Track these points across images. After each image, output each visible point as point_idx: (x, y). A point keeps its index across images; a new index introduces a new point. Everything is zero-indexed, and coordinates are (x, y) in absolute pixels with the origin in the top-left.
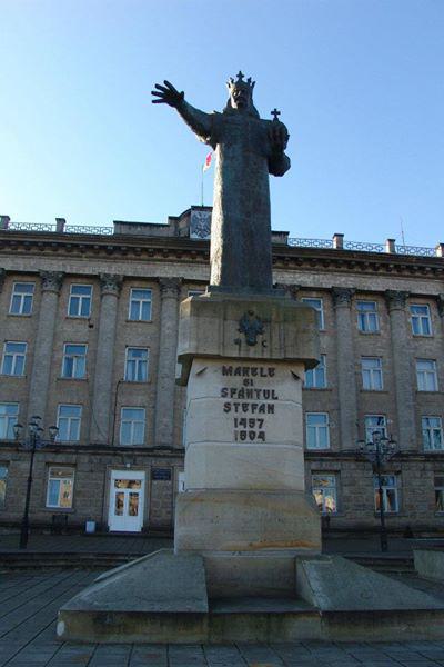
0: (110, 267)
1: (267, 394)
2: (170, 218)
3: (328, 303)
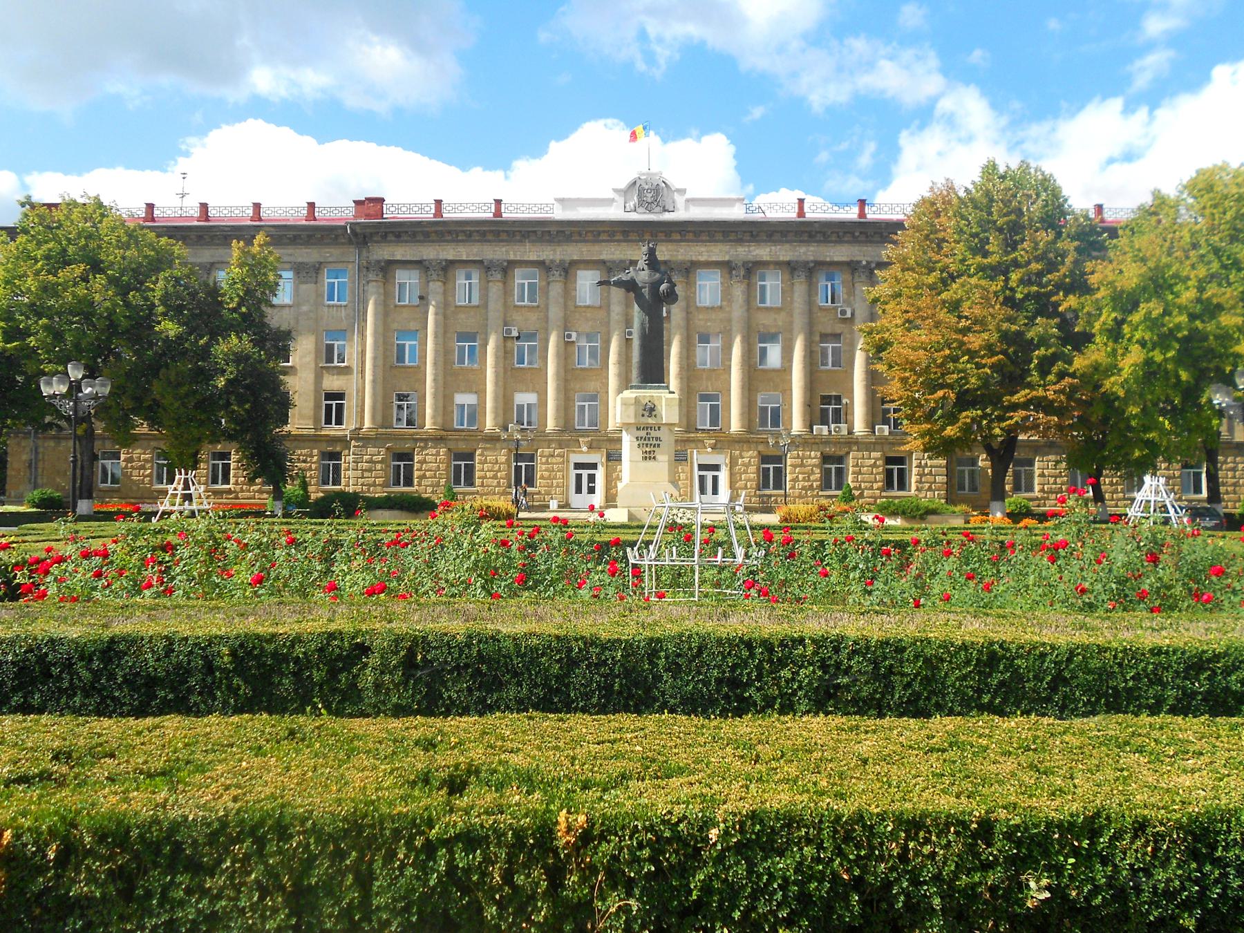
0: (554, 251)
1: (657, 439)
2: (615, 190)
3: (787, 277)
